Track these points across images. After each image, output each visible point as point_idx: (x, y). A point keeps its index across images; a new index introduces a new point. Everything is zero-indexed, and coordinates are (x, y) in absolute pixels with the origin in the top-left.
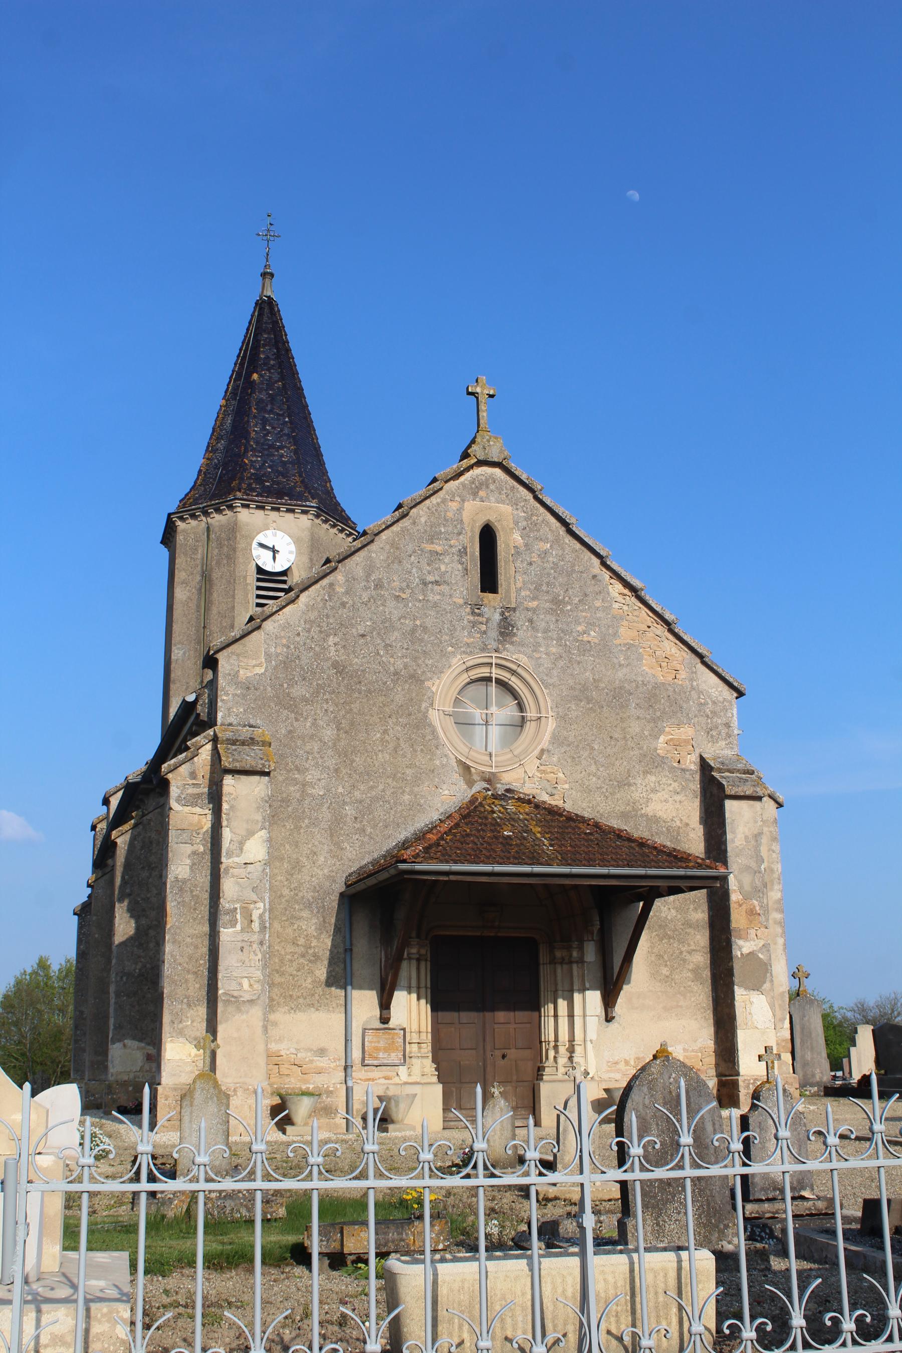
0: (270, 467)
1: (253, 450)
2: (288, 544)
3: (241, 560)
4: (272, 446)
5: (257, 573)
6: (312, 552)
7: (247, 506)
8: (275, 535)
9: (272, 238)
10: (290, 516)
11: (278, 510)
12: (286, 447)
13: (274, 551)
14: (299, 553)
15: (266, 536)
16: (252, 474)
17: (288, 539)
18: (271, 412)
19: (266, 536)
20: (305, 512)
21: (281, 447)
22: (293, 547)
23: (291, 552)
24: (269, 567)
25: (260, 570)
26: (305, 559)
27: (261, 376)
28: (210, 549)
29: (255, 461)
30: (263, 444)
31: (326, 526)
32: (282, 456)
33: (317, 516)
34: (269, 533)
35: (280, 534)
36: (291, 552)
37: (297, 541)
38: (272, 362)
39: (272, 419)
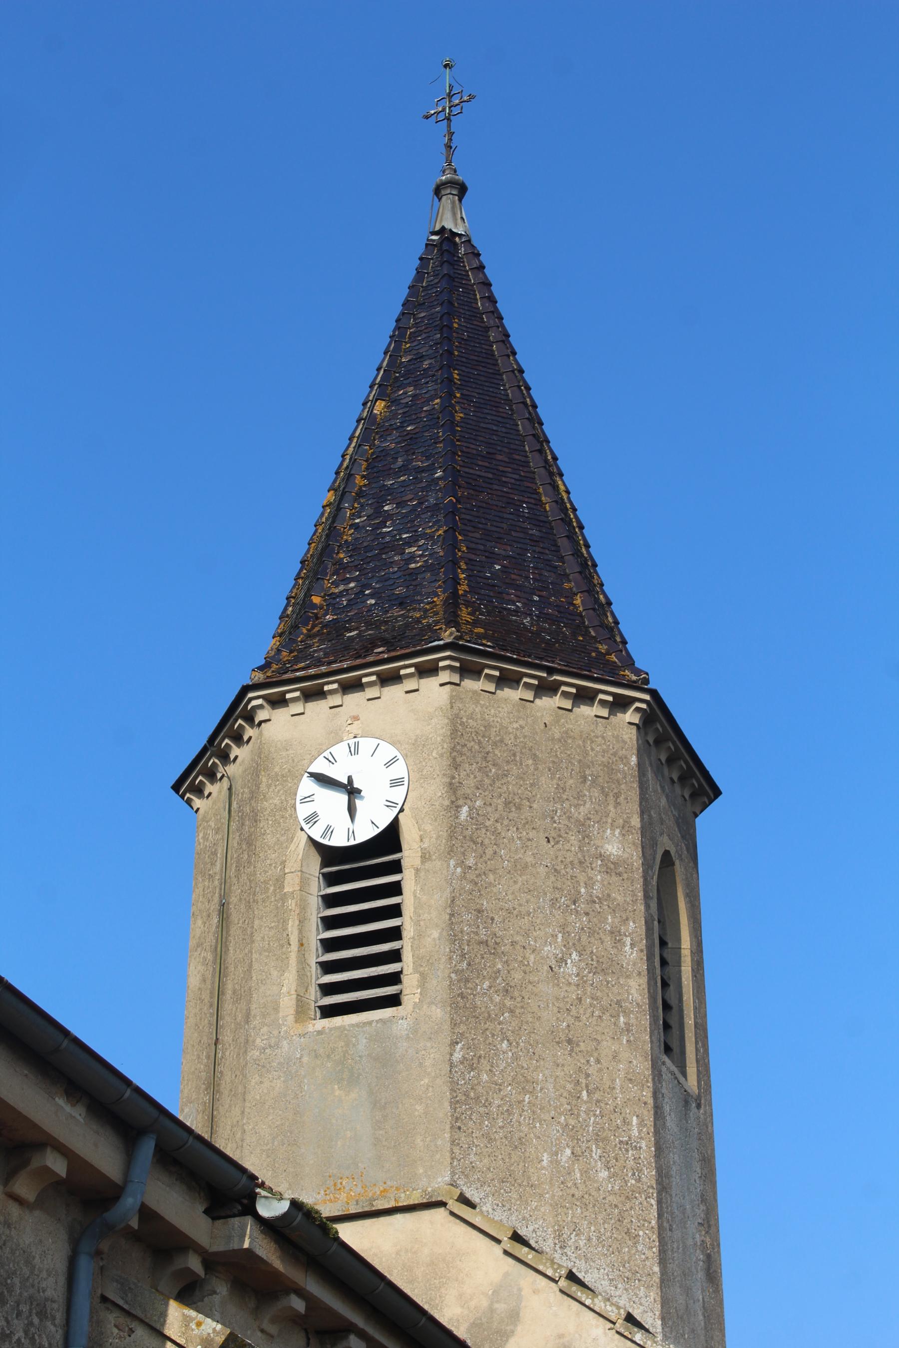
0: (371, 596)
1: (340, 568)
2: (388, 764)
3: (270, 839)
4: (384, 548)
5: (325, 863)
6: (456, 766)
7: (278, 702)
8: (354, 751)
9: (456, 111)
10: (394, 692)
11: (355, 686)
12: (424, 536)
13: (352, 791)
14: (418, 775)
15: (332, 761)
16: (326, 625)
17: (388, 751)
18: (404, 469)
19: (332, 761)
20: (427, 671)
21: (408, 543)
22: (400, 770)
23: (396, 783)
24: (339, 840)
25: (329, 855)
26: (436, 789)
27: (394, 402)
28: (231, 836)
29: (341, 594)
30: (368, 549)
31: (512, 695)
32: (412, 558)
33: (468, 671)
34: (340, 750)
35: (368, 745)
36: (396, 783)
37: (413, 749)
38: (426, 364)
39: (403, 484)
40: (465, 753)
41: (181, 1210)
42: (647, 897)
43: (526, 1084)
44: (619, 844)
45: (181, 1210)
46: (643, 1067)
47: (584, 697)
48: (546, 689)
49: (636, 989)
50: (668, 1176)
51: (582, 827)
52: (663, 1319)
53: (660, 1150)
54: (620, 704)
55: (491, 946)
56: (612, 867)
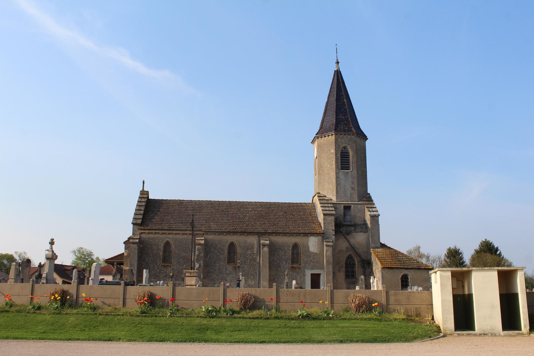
40: (319, 147)
41: (198, 232)
42: (336, 155)
43: (324, 180)
44: (333, 151)
45: (201, 232)
46: (334, 174)
47: (329, 136)
48: (325, 137)
49: (334, 166)
50: (340, 183)
51: (329, 150)
52: (336, 199)
53: (337, 181)
54: (332, 135)
55: (321, 167)
56: (332, 153)
